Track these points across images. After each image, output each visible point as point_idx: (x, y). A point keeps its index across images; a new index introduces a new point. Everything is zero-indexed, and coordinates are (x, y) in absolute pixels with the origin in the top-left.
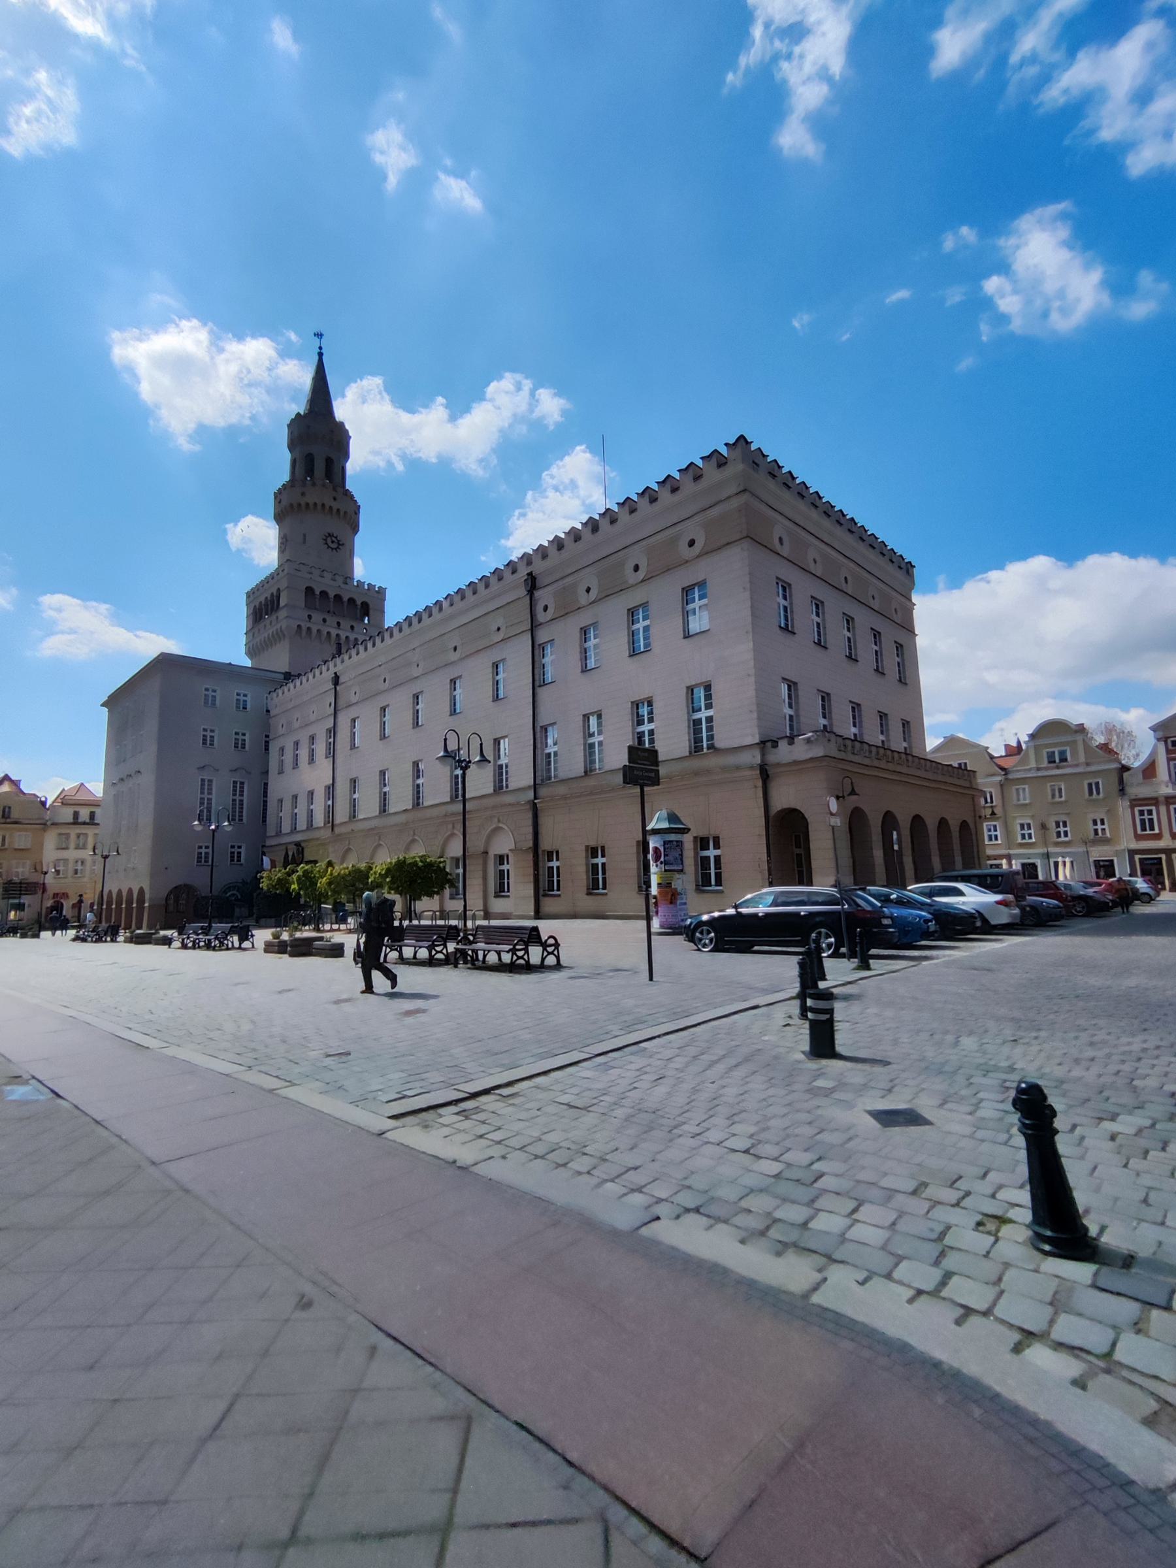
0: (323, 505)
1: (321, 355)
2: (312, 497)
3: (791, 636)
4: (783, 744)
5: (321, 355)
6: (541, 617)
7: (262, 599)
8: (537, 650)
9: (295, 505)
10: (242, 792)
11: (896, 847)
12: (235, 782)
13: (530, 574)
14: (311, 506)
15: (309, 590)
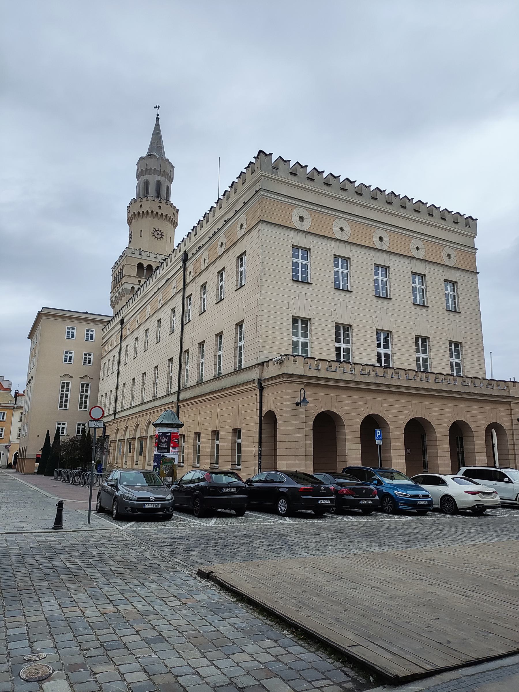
0: (152, 212)
1: (158, 119)
2: (147, 206)
3: (307, 286)
4: (271, 363)
5: (158, 119)
6: (188, 280)
7: (117, 272)
8: (186, 299)
9: (136, 213)
10: (87, 390)
11: (379, 442)
12: (83, 384)
13: (185, 251)
14: (145, 212)
15: (140, 266)
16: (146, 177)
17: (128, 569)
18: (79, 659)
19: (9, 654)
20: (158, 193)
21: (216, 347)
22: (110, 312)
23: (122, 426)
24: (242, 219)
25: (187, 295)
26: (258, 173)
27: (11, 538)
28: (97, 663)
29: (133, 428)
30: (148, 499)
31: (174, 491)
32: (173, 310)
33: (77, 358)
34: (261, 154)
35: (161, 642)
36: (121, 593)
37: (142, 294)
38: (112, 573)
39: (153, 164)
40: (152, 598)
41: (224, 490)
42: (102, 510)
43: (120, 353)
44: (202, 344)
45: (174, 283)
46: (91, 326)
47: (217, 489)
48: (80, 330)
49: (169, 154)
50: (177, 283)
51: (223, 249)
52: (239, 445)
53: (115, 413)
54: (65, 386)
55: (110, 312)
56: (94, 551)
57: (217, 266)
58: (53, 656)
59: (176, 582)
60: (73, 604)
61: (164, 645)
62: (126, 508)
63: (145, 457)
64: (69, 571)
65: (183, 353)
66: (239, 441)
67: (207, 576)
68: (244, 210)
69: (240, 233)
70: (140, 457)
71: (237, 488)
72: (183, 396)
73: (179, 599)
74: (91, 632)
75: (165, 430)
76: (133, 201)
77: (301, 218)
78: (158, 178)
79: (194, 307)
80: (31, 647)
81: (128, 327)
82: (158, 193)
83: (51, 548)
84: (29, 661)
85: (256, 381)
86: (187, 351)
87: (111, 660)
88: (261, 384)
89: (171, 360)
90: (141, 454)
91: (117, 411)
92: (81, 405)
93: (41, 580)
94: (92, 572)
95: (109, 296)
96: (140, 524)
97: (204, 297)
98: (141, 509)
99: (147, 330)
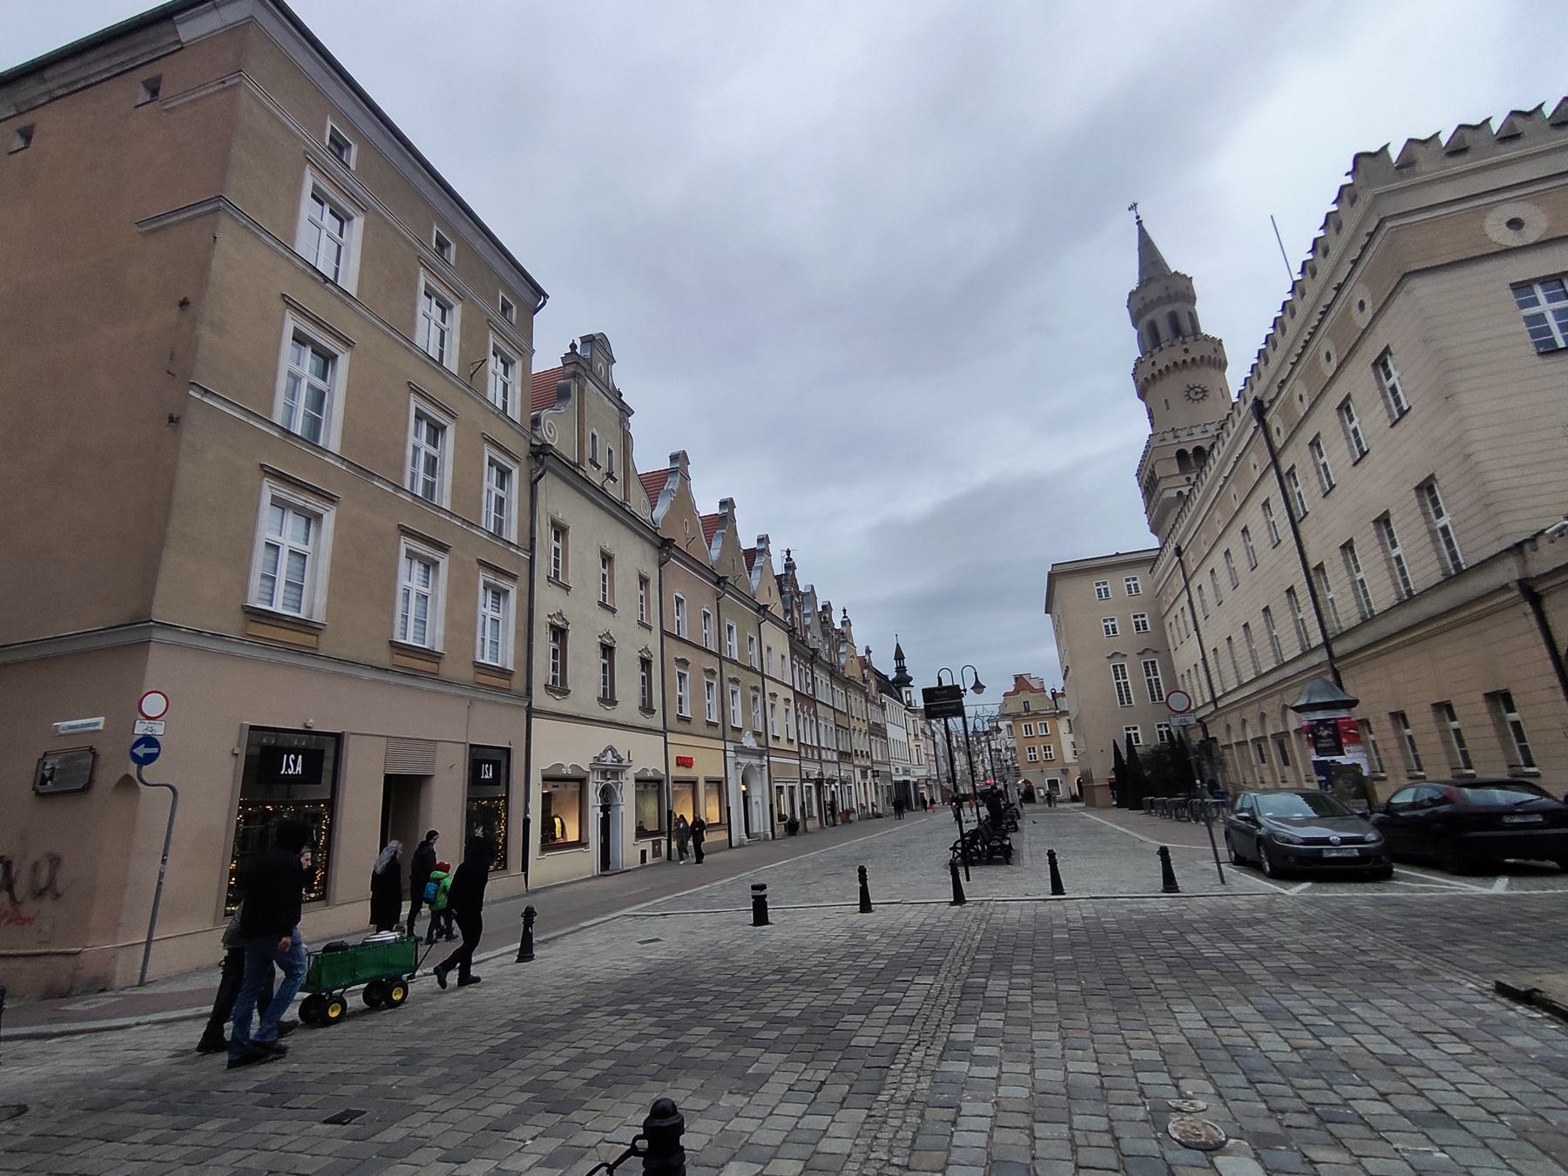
1: (1139, 223)
2: (1163, 360)
4: (1542, 541)
5: (1139, 223)
6: (1278, 444)
8: (1285, 479)
15: (1181, 455)
16: (1148, 317)
17: (1323, 970)
18: (1270, 1126)
19: (1142, 1093)
20: (1177, 330)
21: (1382, 544)
22: (1153, 542)
23: (1234, 719)
24: (1358, 291)
25: (1285, 470)
26: (1366, 197)
27: (1101, 905)
28: (1311, 1143)
29: (1256, 721)
30: (1326, 841)
31: (1379, 825)
32: (1266, 505)
33: (1124, 623)
34: (1363, 160)
35: (1449, 1127)
36: (1324, 1011)
37: (1199, 496)
38: (1293, 973)
39: (1154, 292)
40: (1398, 1031)
41: (1507, 820)
42: (1239, 861)
43: (1190, 601)
44: (1348, 547)
45: (1253, 459)
46: (1130, 573)
47: (1492, 817)
48: (1116, 583)
49: (1175, 263)
50: (1258, 458)
51: (1334, 363)
52: (1516, 725)
53: (1215, 700)
54: (1119, 671)
55: (1153, 542)
56: (1248, 932)
57: (1334, 397)
58: (1216, 1105)
59: (1450, 1004)
60: (1231, 1022)
61: (1457, 1136)
62: (1286, 857)
63: (1296, 768)
64: (1208, 962)
65: (1314, 573)
66: (1513, 716)
67: (1529, 998)
68: (1357, 274)
69: (1362, 320)
70: (1286, 769)
71: (1544, 812)
72: (1338, 649)
73: (1466, 1041)
74: (1280, 1078)
75: (1320, 715)
76: (1139, 362)
77: (1515, 224)
78: (1168, 309)
79: (1307, 488)
80: (1177, 1087)
81: (1191, 560)
82: (1177, 330)
83: (1167, 922)
84: (1178, 1110)
85: (1514, 585)
86: (1320, 568)
87: (1338, 1143)
88: (1531, 589)
89: (1290, 591)
90: (1286, 763)
91: (1218, 695)
92: (1153, 696)
93: (1164, 975)
94: (1251, 968)
95: (1145, 518)
96: (1324, 887)
97: (1321, 461)
98: (1317, 857)
99: (1227, 553)
